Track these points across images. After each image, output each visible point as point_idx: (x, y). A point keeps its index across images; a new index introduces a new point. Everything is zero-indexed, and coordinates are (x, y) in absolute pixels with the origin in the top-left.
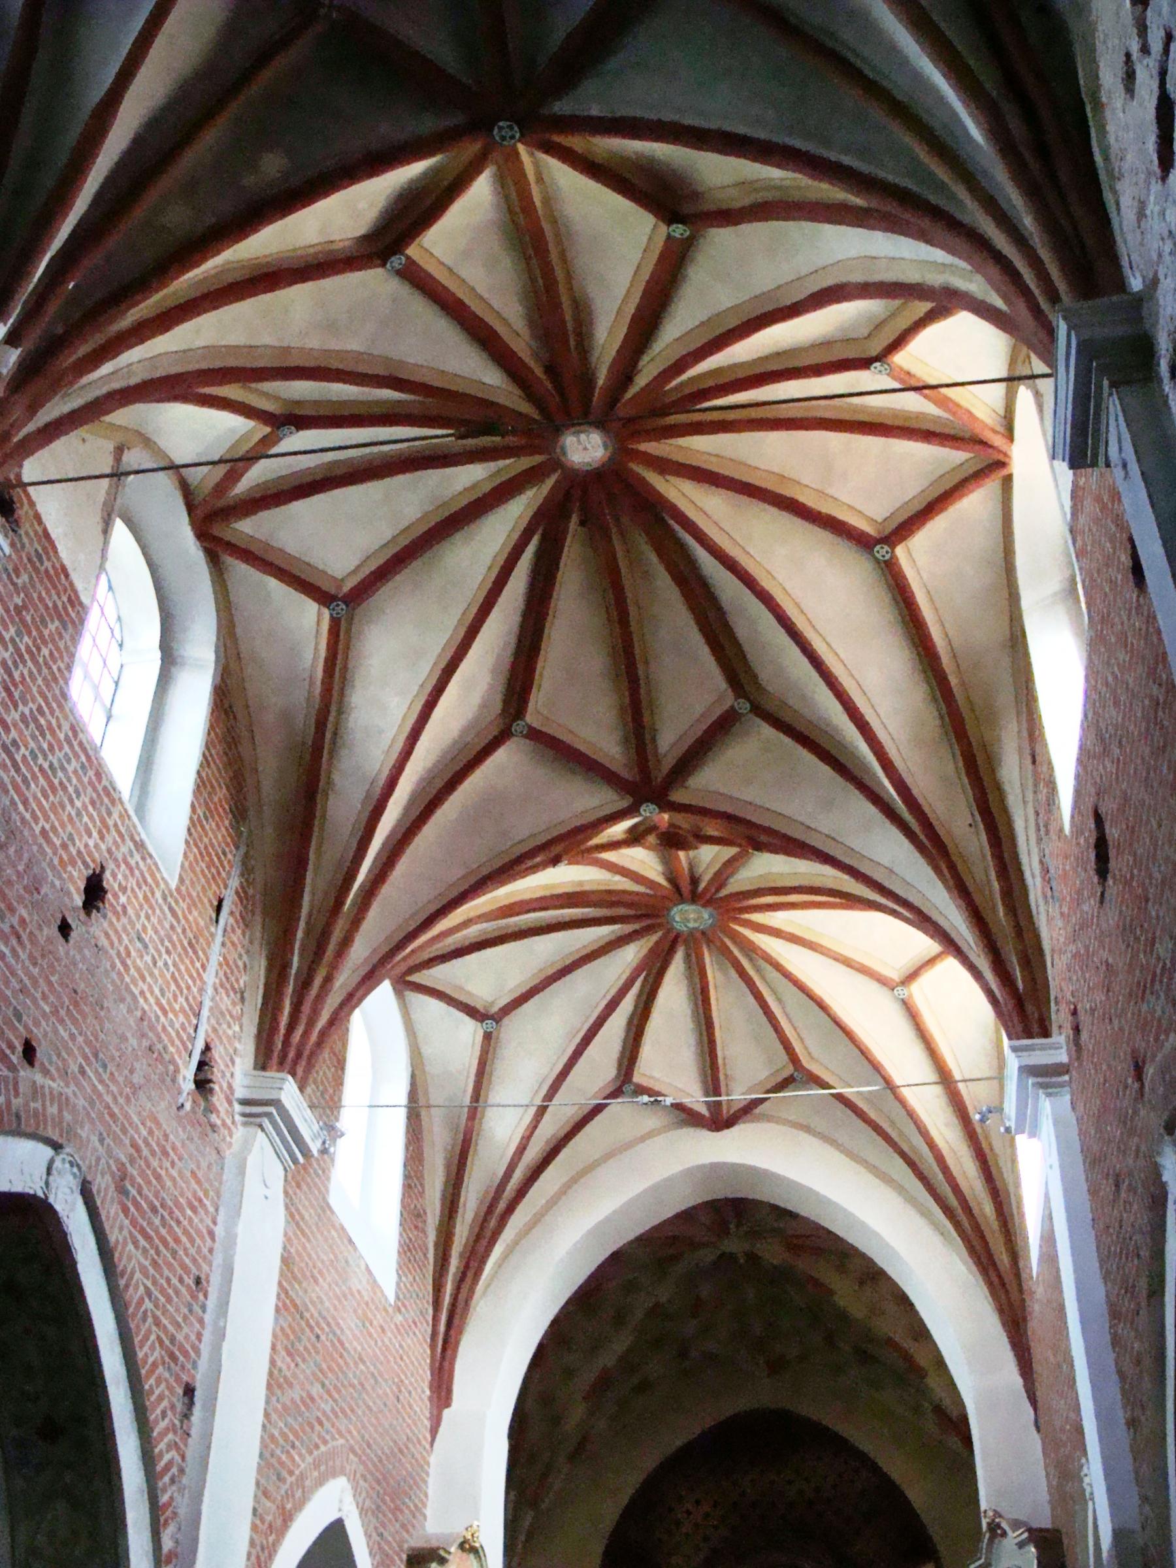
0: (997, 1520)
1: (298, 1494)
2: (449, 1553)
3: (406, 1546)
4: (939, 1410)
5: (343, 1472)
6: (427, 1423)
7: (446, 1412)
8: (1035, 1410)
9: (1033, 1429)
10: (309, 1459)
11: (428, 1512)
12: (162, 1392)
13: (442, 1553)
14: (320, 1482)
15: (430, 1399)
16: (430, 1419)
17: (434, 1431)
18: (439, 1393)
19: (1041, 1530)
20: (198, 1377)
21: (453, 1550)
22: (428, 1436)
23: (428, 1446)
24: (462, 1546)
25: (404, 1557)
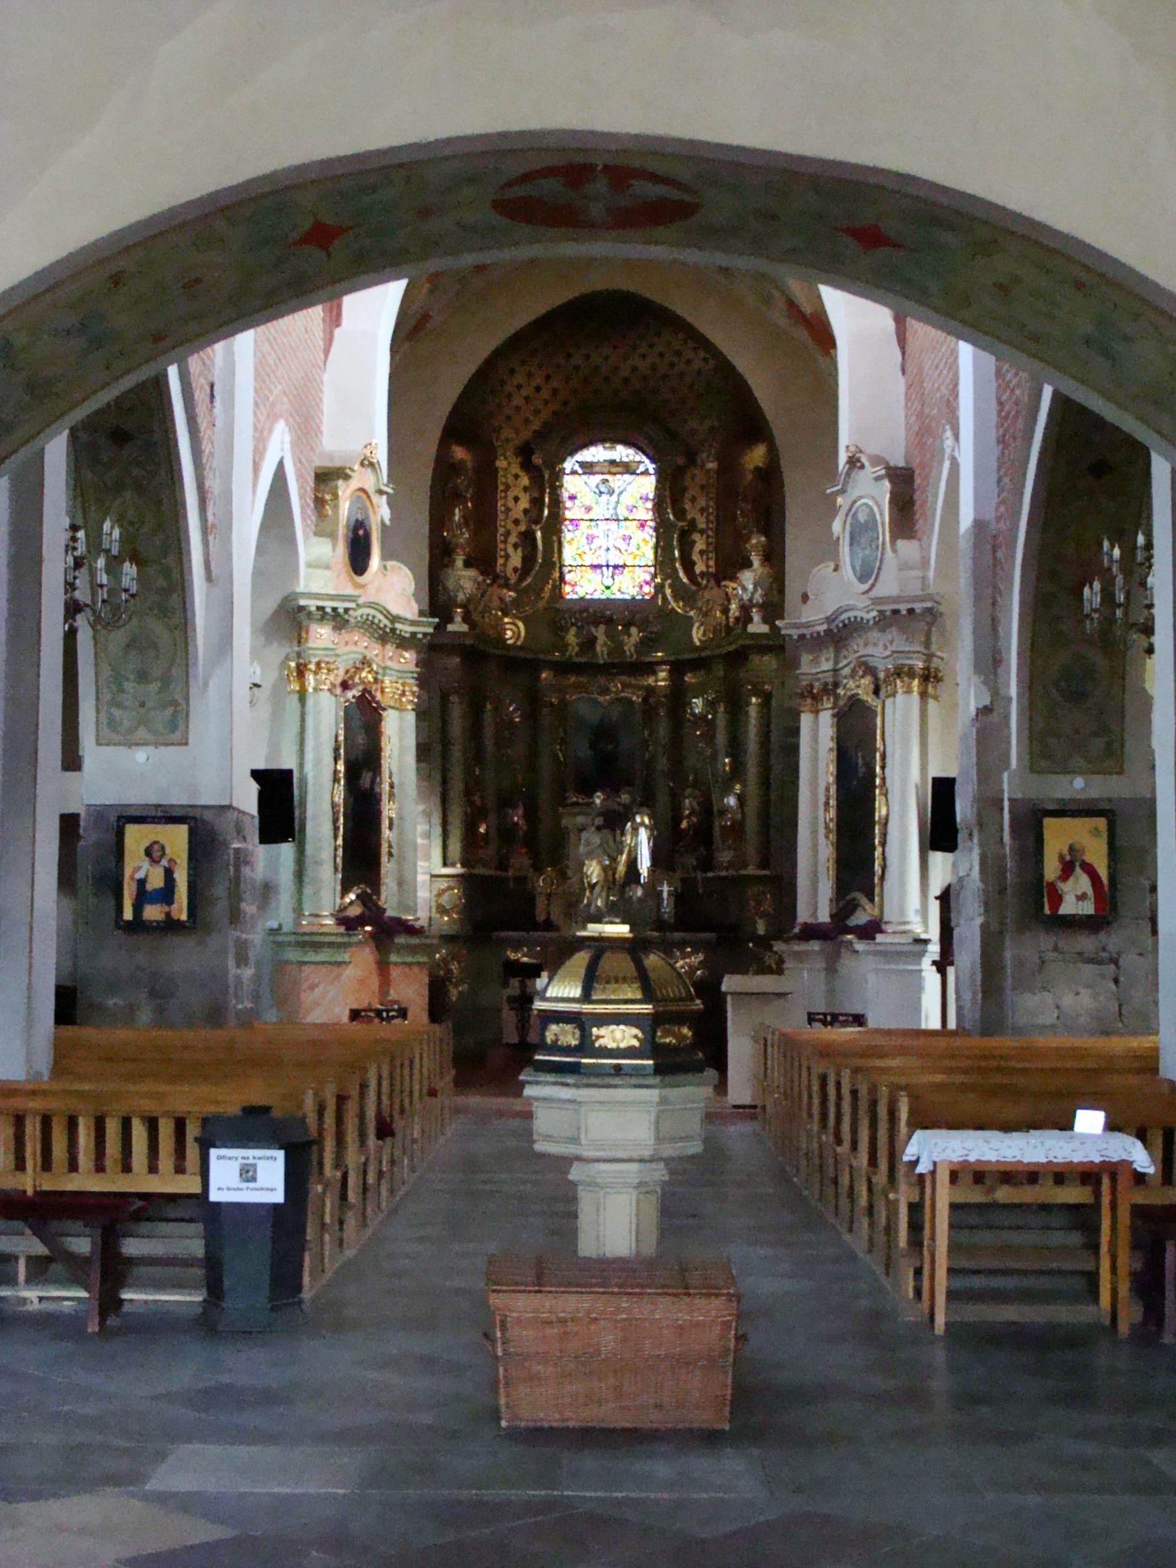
0: (858, 455)
1: (261, 447)
2: (353, 470)
3: (314, 465)
4: (792, 305)
5: (281, 416)
6: (322, 344)
7: (338, 332)
8: (903, 353)
9: (900, 373)
10: (265, 413)
11: (324, 429)
12: (200, 396)
13: (348, 471)
14: (271, 431)
15: (324, 320)
16: (324, 340)
17: (327, 352)
18: (331, 312)
19: (897, 468)
20: (216, 373)
21: (356, 468)
22: (322, 356)
23: (321, 364)
24: (362, 464)
25: (313, 475)
